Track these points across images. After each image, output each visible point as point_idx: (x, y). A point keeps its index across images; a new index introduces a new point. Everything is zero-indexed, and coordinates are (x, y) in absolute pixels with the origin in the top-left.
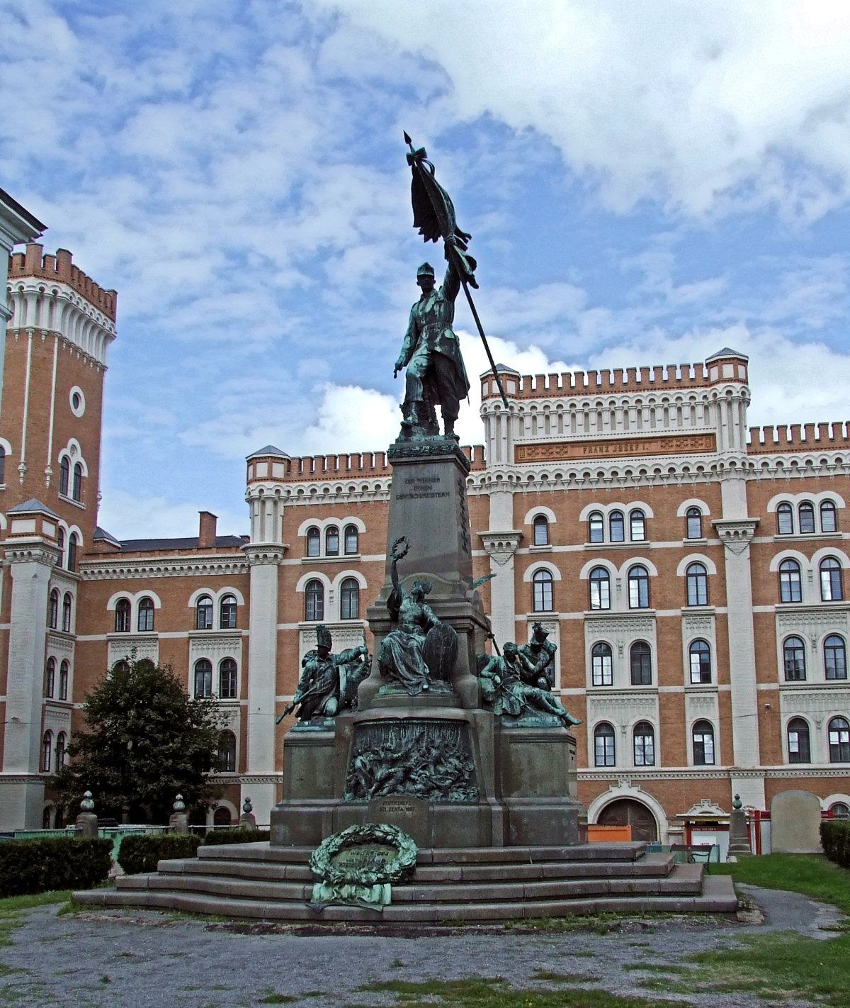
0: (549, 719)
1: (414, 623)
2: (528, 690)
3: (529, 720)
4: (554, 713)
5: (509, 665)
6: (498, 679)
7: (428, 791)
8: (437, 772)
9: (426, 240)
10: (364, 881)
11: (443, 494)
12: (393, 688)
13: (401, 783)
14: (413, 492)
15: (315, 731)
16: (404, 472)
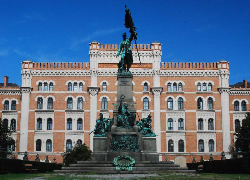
2: (148, 129)
6: (141, 126)
7: (131, 149)
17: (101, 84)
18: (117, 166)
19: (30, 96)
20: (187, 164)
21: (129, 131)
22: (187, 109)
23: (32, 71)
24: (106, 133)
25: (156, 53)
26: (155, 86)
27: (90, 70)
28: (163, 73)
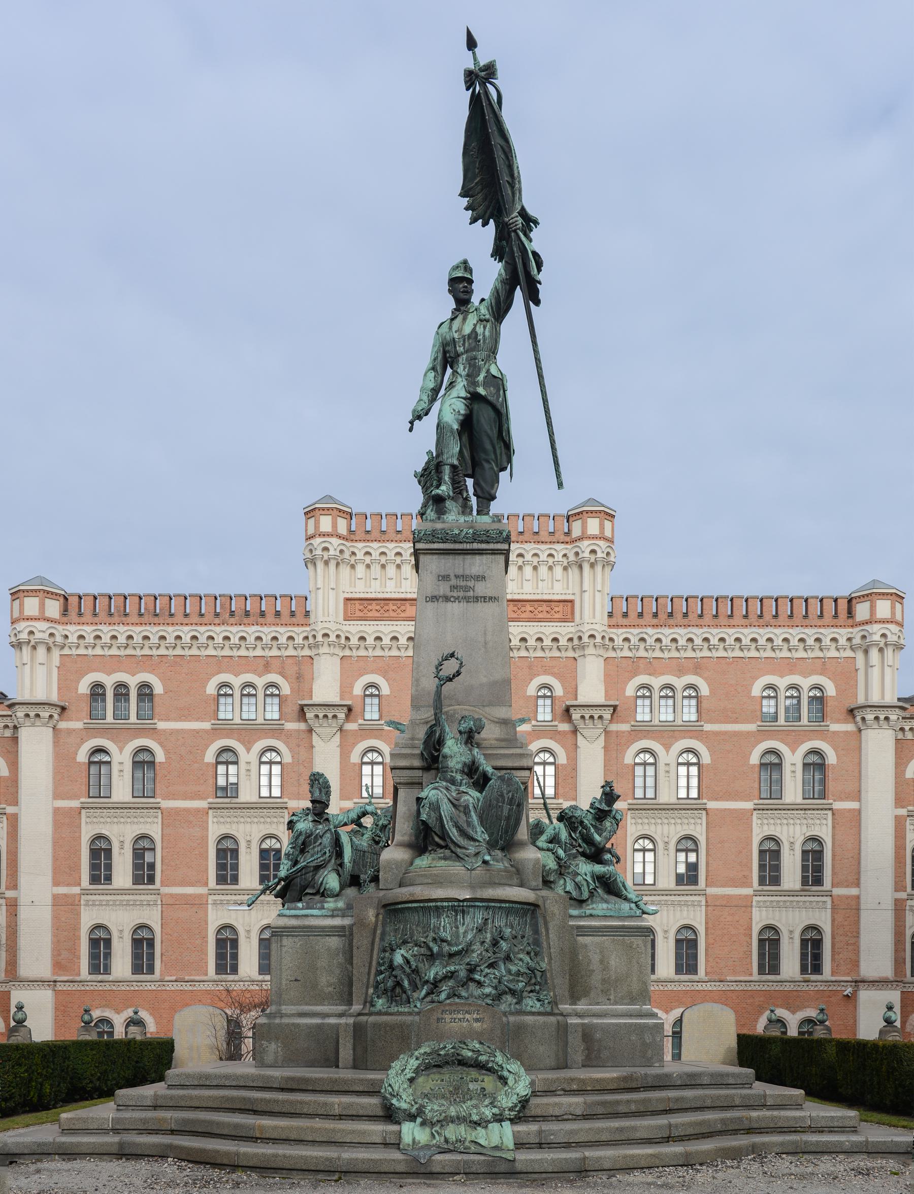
0: (626, 906)
1: (463, 772)
2: (599, 869)
3: (599, 907)
4: (626, 899)
5: (573, 835)
6: (561, 852)
7: (498, 997)
8: (509, 972)
9: (473, 221)
10: (475, 1118)
11: (491, 598)
12: (440, 858)
13: (462, 986)
14: (449, 594)
15: (318, 916)
16: (431, 563)
17: (358, 690)
18: (412, 1118)
19: (56, 742)
20: (738, 1035)
21: (493, 884)
22: (716, 799)
23: (60, 630)
24: (351, 892)
25: (593, 552)
26: (581, 700)
27: (308, 629)
28: (618, 641)
